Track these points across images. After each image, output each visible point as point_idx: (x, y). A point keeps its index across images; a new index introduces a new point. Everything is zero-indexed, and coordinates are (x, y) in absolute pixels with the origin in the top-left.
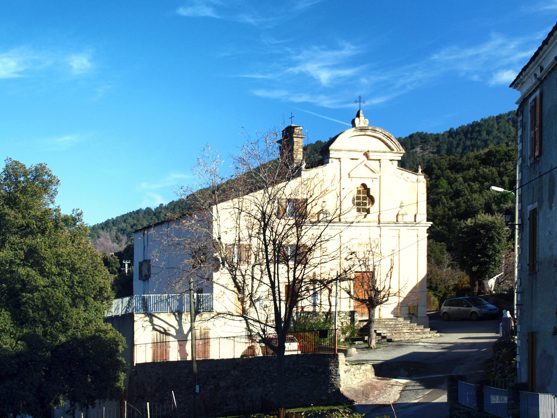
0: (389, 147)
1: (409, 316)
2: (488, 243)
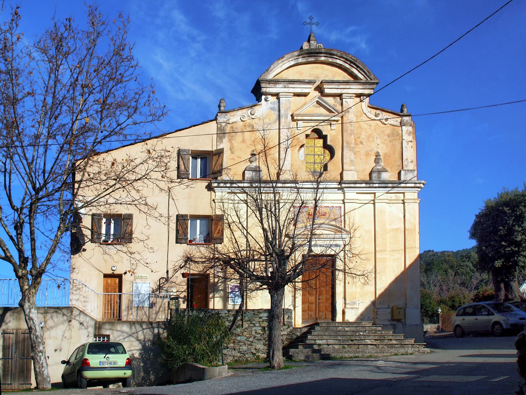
0: (351, 74)
1: (392, 323)
2: (515, 225)
